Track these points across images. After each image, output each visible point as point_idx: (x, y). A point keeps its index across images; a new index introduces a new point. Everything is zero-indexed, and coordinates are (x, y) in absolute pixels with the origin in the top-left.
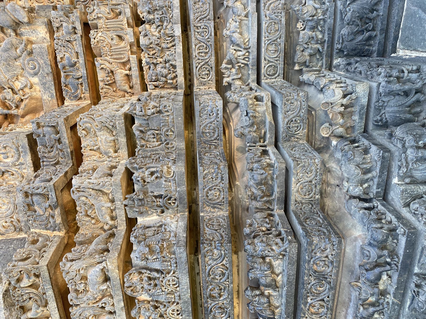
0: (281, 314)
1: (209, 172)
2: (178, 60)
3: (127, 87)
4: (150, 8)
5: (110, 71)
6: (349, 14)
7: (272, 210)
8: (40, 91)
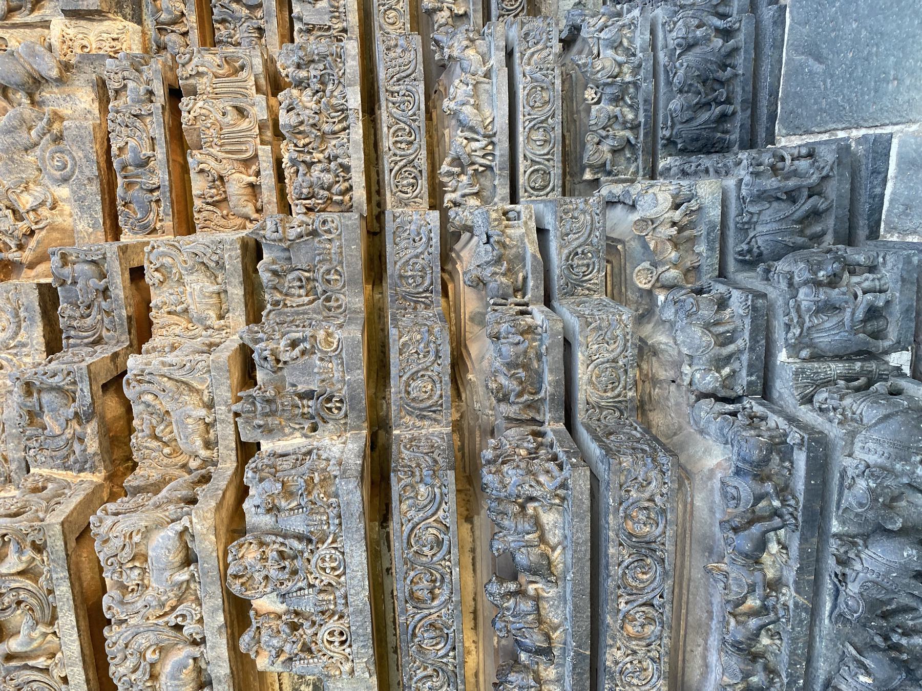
0: (565, 644)
1: (410, 339)
2: (354, 156)
3: (250, 210)
4: (300, 58)
5: (216, 177)
6: (681, 72)
7: (542, 423)
8: (71, 215)
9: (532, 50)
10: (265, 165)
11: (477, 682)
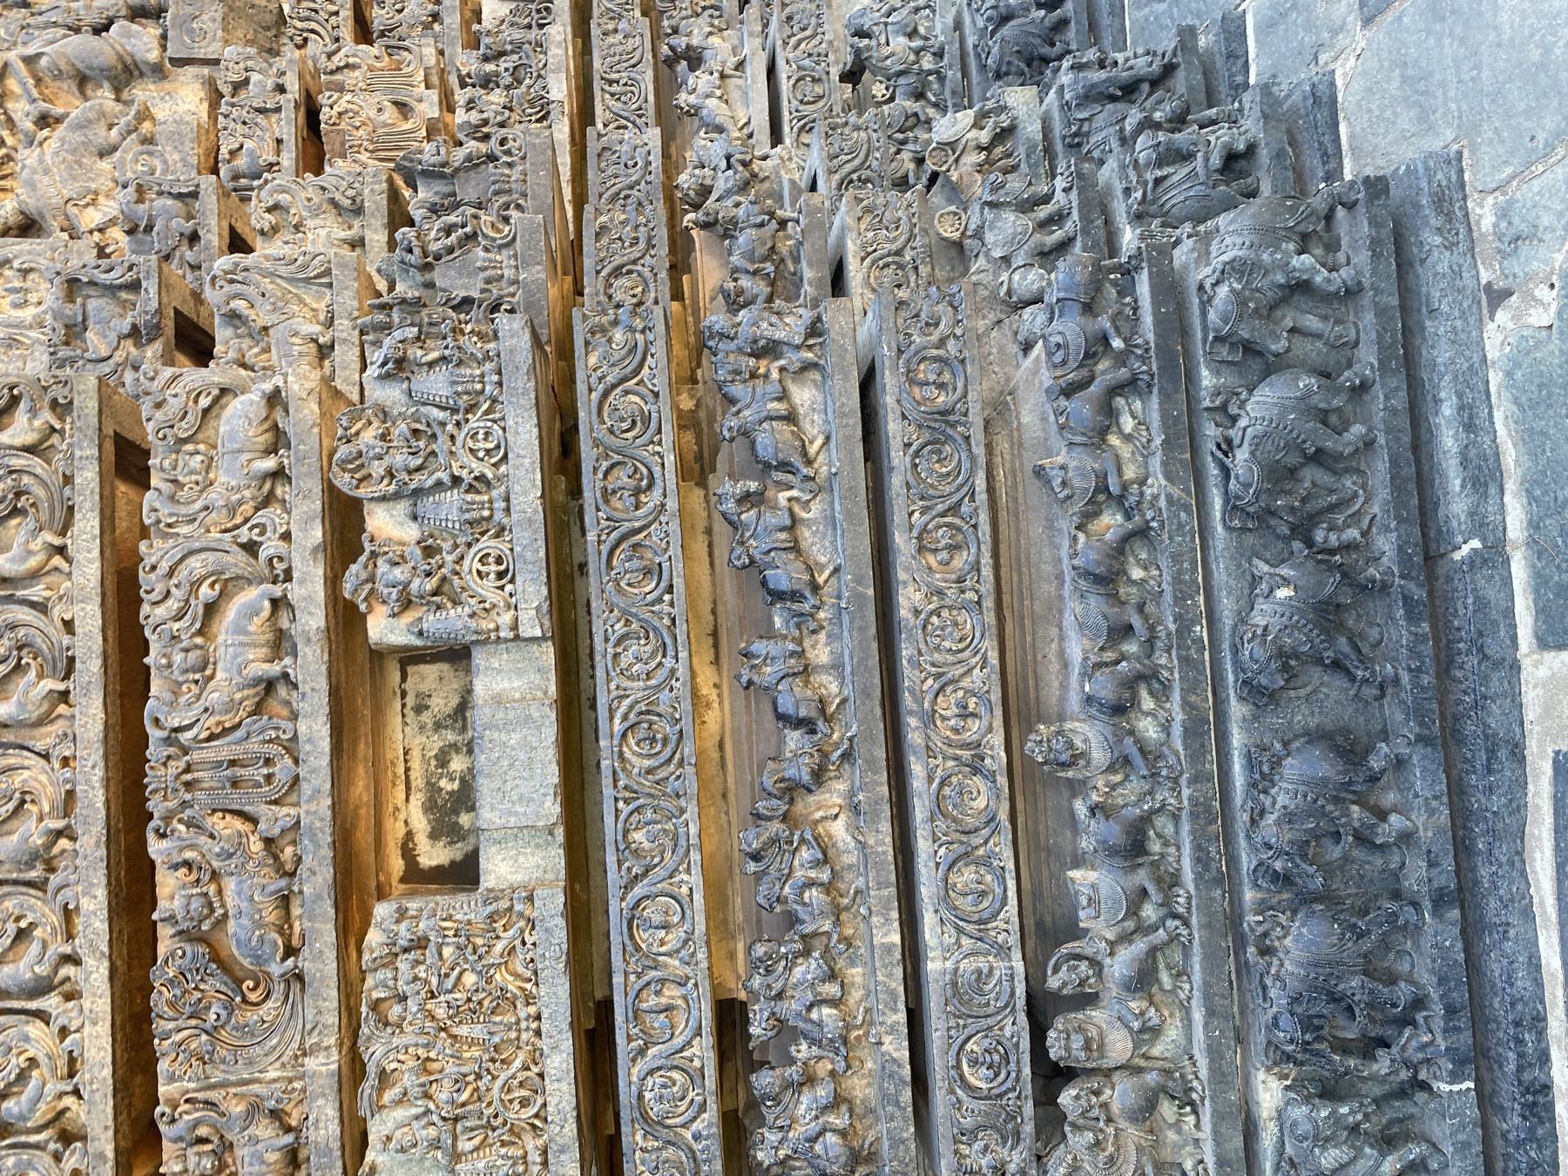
1: (612, 220)
6: (995, 50)
11: (723, 758)
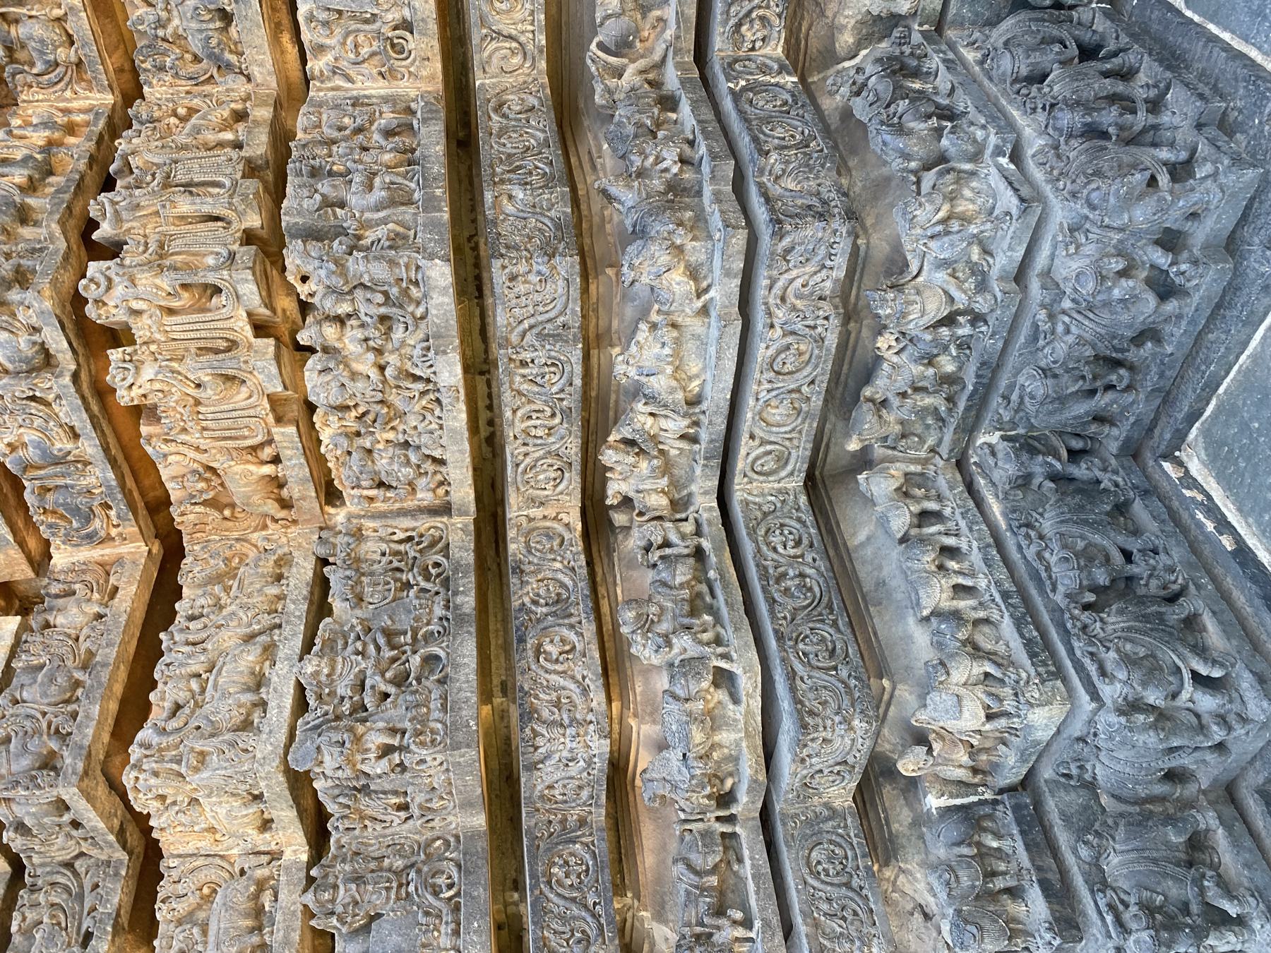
3: (272, 507)
6: (1061, 348)
9: (794, 273)
10: (289, 452)
